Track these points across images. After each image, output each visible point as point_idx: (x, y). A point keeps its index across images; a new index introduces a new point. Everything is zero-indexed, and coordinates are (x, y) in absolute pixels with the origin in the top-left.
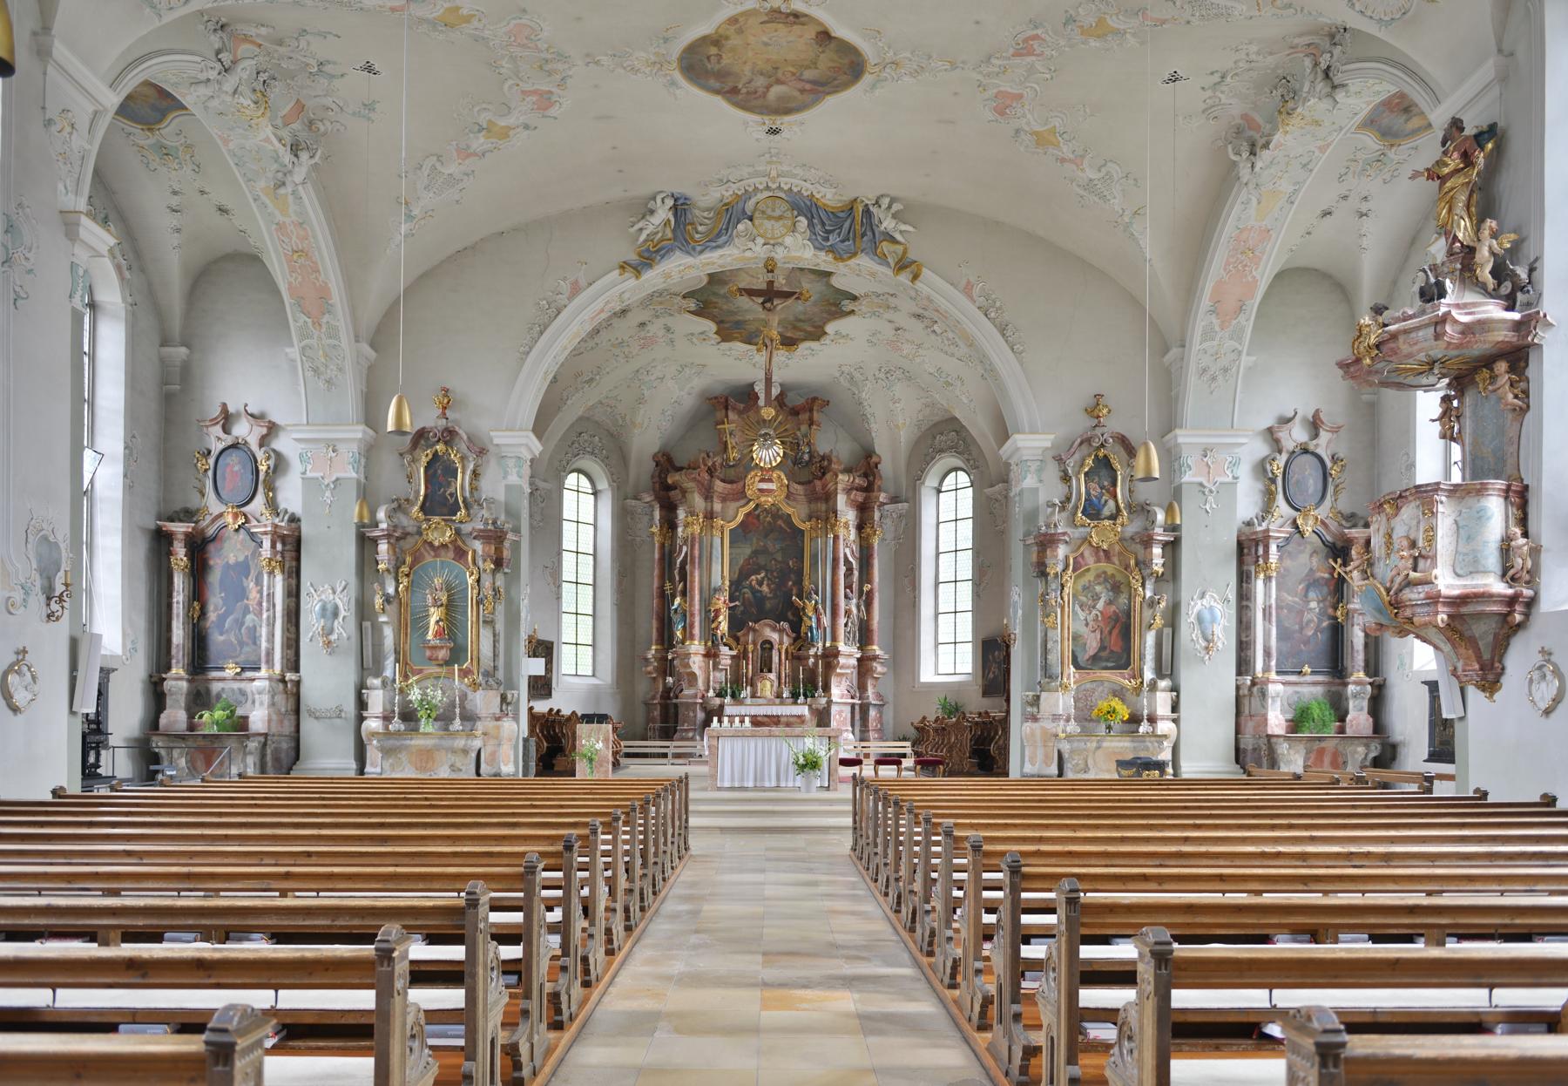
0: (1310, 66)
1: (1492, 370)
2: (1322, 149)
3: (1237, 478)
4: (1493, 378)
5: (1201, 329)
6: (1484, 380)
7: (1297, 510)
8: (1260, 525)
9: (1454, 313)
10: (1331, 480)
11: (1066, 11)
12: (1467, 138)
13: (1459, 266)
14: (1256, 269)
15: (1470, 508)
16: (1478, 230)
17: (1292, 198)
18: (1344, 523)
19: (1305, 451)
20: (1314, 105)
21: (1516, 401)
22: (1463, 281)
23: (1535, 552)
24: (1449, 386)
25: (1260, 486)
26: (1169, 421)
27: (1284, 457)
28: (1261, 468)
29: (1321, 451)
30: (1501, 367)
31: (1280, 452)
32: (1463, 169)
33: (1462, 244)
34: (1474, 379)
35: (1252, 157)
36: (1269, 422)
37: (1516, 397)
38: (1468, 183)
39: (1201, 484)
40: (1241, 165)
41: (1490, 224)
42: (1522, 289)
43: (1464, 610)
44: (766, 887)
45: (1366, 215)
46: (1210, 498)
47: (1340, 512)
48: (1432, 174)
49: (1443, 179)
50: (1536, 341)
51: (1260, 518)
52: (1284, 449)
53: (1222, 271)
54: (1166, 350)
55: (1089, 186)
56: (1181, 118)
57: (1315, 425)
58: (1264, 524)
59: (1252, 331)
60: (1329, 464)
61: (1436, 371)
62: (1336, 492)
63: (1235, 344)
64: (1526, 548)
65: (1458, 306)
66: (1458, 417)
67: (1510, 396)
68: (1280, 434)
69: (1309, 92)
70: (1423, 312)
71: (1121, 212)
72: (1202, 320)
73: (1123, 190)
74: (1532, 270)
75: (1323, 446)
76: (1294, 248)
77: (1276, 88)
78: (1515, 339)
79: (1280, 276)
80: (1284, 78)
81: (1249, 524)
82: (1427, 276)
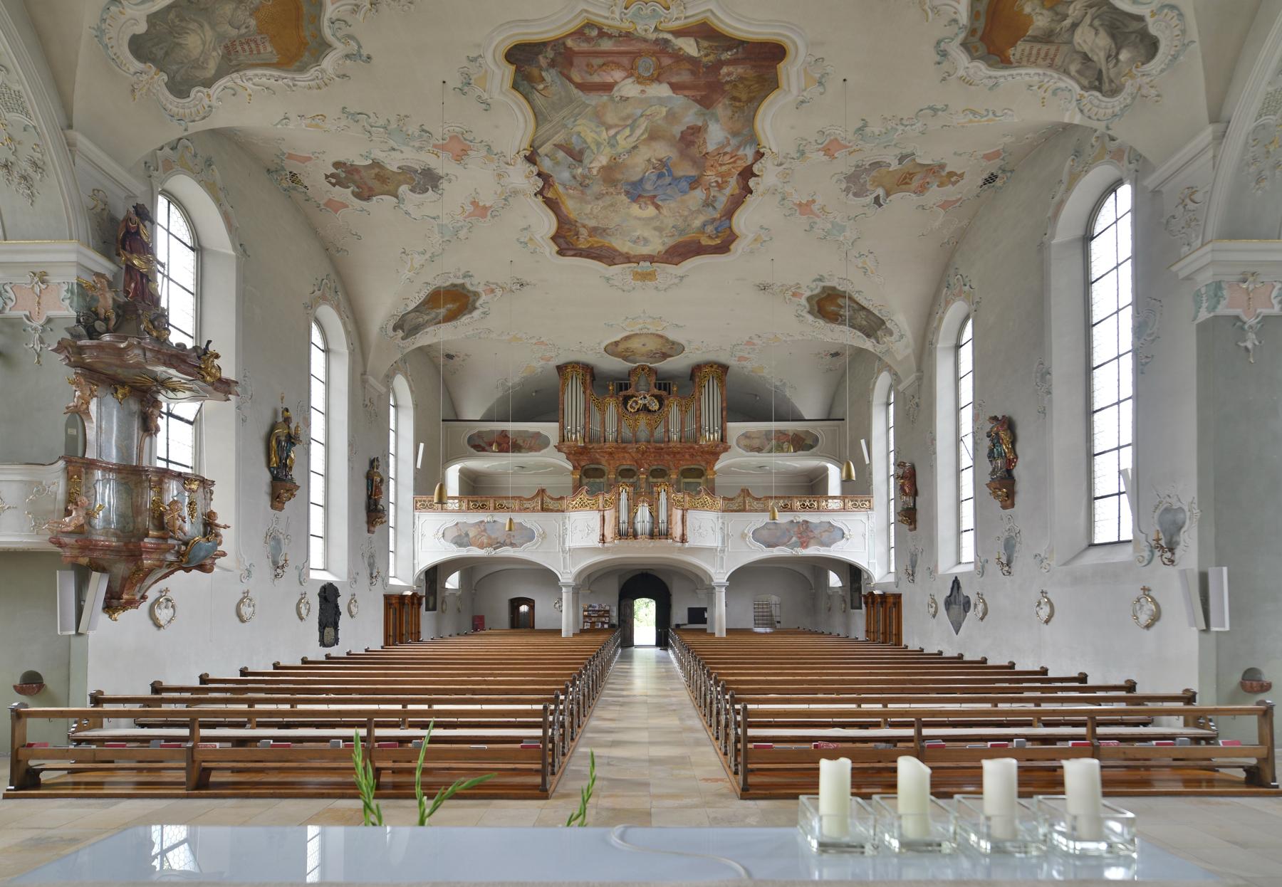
44: (647, 740)
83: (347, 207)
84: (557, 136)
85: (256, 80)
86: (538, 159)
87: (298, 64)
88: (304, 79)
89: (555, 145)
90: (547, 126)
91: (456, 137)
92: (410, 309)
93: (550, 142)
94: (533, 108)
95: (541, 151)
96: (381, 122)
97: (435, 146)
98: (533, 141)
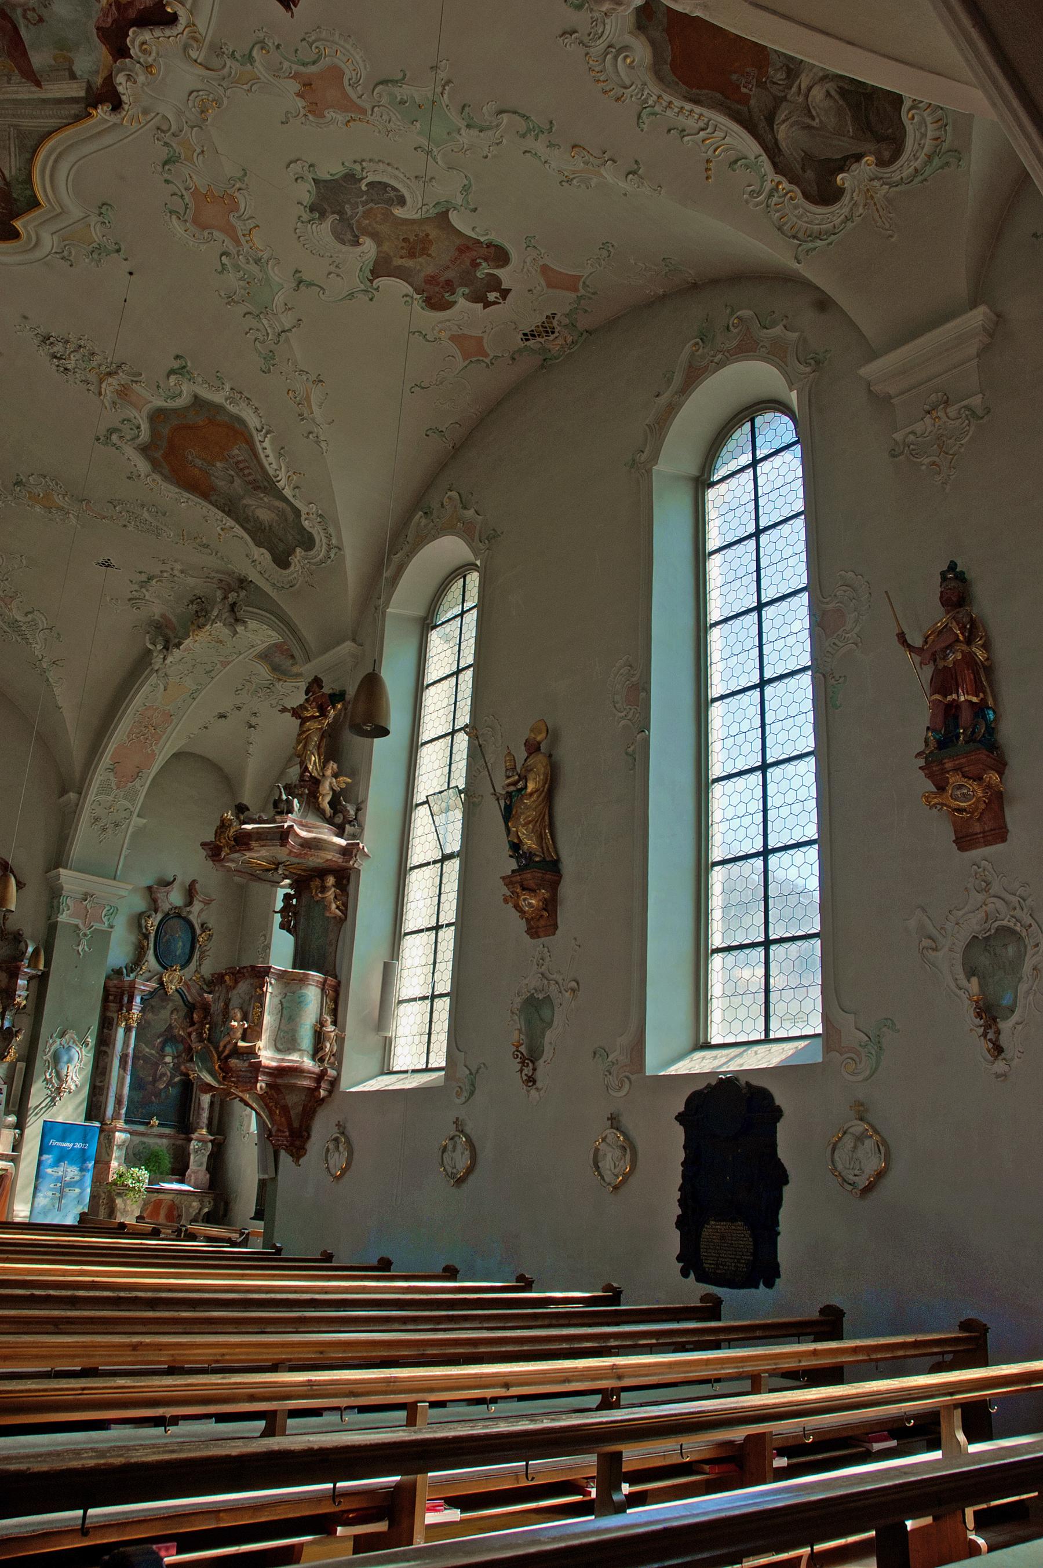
0: (221, 597)
1: (323, 881)
2: (224, 664)
3: (112, 927)
4: (324, 889)
5: (98, 782)
6: (317, 888)
7: (165, 968)
8: (128, 975)
9: (295, 827)
10: (198, 946)
11: (18, 475)
12: (323, 694)
13: (307, 791)
14: (156, 744)
15: (294, 993)
16: (324, 767)
17: (195, 695)
18: (205, 987)
19: (179, 916)
20: (219, 629)
21: (337, 911)
22: (308, 803)
23: (340, 1040)
24: (291, 886)
25: (133, 938)
26: (58, 859)
27: (159, 916)
28: (138, 921)
29: (193, 918)
30: (331, 880)
31: (156, 912)
32: (318, 717)
33: (311, 774)
34: (309, 885)
35: (164, 651)
36: (148, 881)
37: (338, 908)
38: (322, 728)
39: (77, 926)
40: (155, 654)
41: (332, 766)
42: (350, 822)
43: (279, 1081)
45: (254, 727)
46: (84, 941)
47: (202, 977)
48: (296, 713)
49: (304, 720)
50: (355, 866)
51: (129, 969)
52: (160, 909)
53: (125, 737)
54: (63, 792)
55: (14, 624)
56: (108, 599)
57: (190, 893)
58: (132, 975)
59: (145, 797)
60: (198, 932)
61: (280, 872)
62: (201, 959)
63: (128, 805)
64: (333, 1034)
65: (302, 825)
66: (295, 914)
67: (334, 906)
68: (159, 895)
69: (217, 616)
70: (274, 822)
71: (40, 658)
72: (100, 776)
73: (45, 639)
74: (358, 810)
75: (196, 913)
76: (192, 736)
77: (192, 604)
78: (340, 860)
79: (177, 756)
80: (200, 598)
81: (118, 972)
82: (281, 792)
83: (545, 269)
84: (20, 97)
85: (274, 466)
86: (99, 81)
87: (237, 425)
88: (253, 421)
89: (38, 84)
90: (27, 124)
91: (195, 222)
92: (751, 147)
93: (43, 96)
94: (30, 161)
95: (76, 90)
96: (254, 323)
97: (238, 242)
98: (78, 118)
